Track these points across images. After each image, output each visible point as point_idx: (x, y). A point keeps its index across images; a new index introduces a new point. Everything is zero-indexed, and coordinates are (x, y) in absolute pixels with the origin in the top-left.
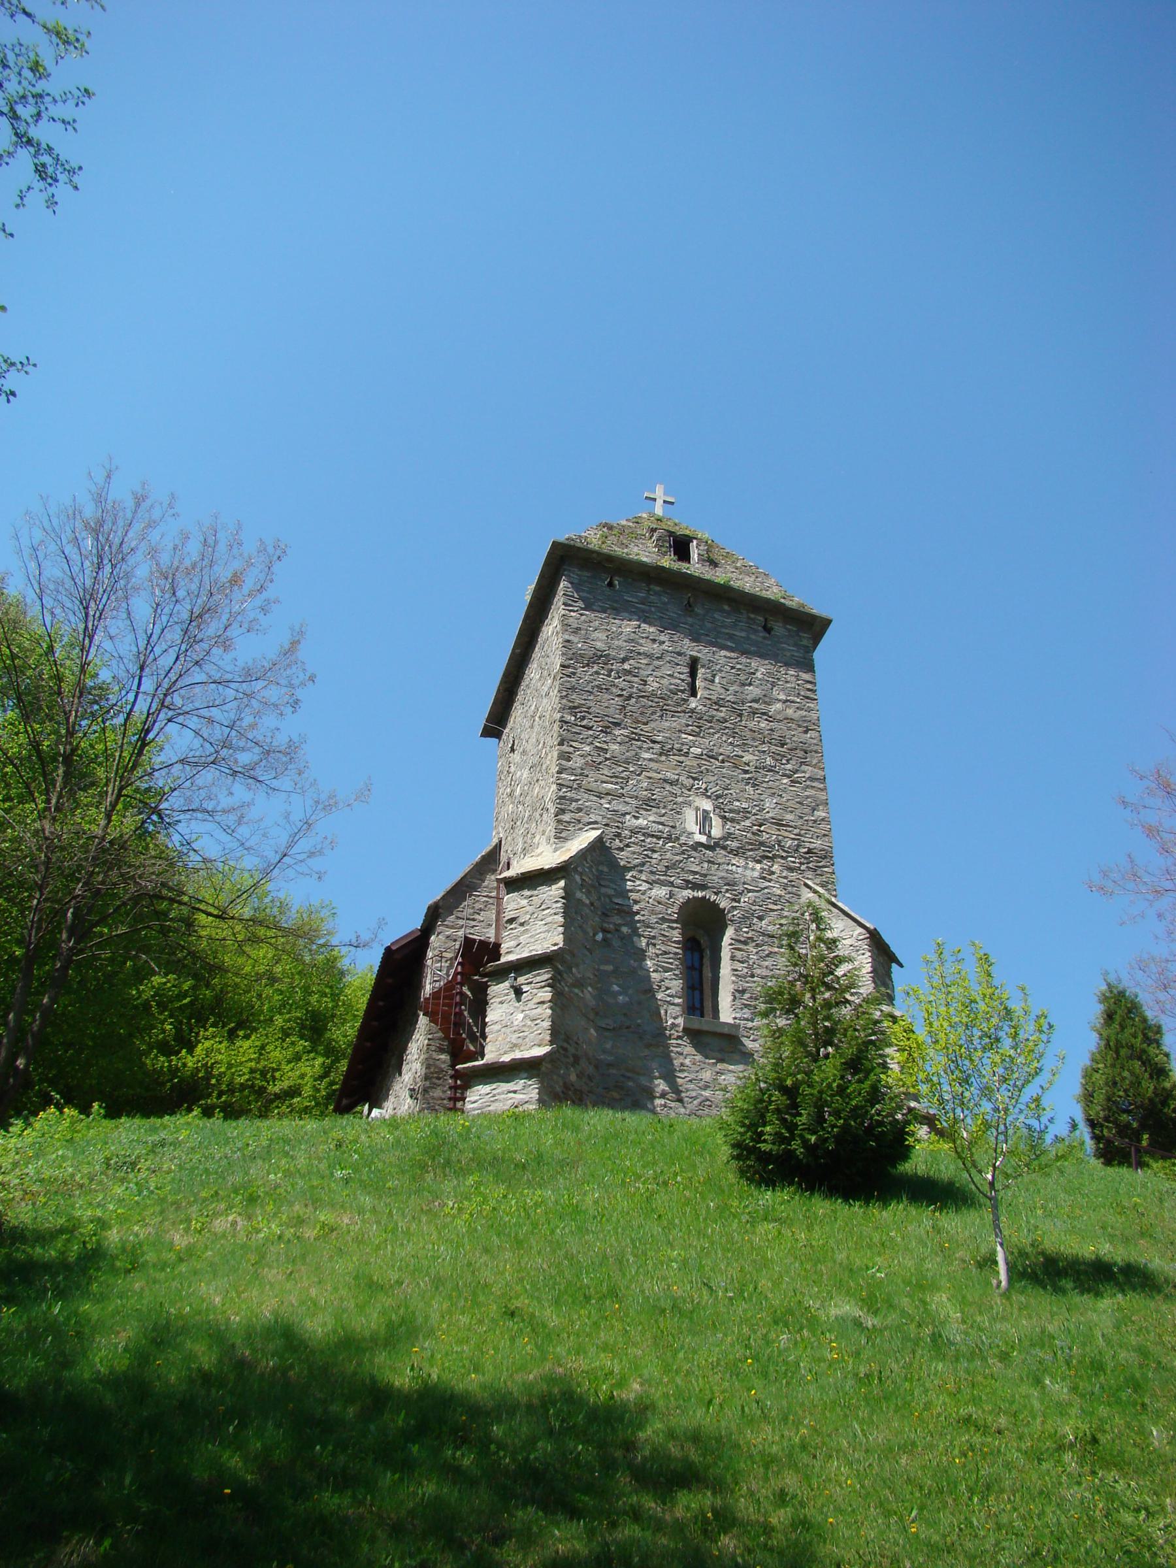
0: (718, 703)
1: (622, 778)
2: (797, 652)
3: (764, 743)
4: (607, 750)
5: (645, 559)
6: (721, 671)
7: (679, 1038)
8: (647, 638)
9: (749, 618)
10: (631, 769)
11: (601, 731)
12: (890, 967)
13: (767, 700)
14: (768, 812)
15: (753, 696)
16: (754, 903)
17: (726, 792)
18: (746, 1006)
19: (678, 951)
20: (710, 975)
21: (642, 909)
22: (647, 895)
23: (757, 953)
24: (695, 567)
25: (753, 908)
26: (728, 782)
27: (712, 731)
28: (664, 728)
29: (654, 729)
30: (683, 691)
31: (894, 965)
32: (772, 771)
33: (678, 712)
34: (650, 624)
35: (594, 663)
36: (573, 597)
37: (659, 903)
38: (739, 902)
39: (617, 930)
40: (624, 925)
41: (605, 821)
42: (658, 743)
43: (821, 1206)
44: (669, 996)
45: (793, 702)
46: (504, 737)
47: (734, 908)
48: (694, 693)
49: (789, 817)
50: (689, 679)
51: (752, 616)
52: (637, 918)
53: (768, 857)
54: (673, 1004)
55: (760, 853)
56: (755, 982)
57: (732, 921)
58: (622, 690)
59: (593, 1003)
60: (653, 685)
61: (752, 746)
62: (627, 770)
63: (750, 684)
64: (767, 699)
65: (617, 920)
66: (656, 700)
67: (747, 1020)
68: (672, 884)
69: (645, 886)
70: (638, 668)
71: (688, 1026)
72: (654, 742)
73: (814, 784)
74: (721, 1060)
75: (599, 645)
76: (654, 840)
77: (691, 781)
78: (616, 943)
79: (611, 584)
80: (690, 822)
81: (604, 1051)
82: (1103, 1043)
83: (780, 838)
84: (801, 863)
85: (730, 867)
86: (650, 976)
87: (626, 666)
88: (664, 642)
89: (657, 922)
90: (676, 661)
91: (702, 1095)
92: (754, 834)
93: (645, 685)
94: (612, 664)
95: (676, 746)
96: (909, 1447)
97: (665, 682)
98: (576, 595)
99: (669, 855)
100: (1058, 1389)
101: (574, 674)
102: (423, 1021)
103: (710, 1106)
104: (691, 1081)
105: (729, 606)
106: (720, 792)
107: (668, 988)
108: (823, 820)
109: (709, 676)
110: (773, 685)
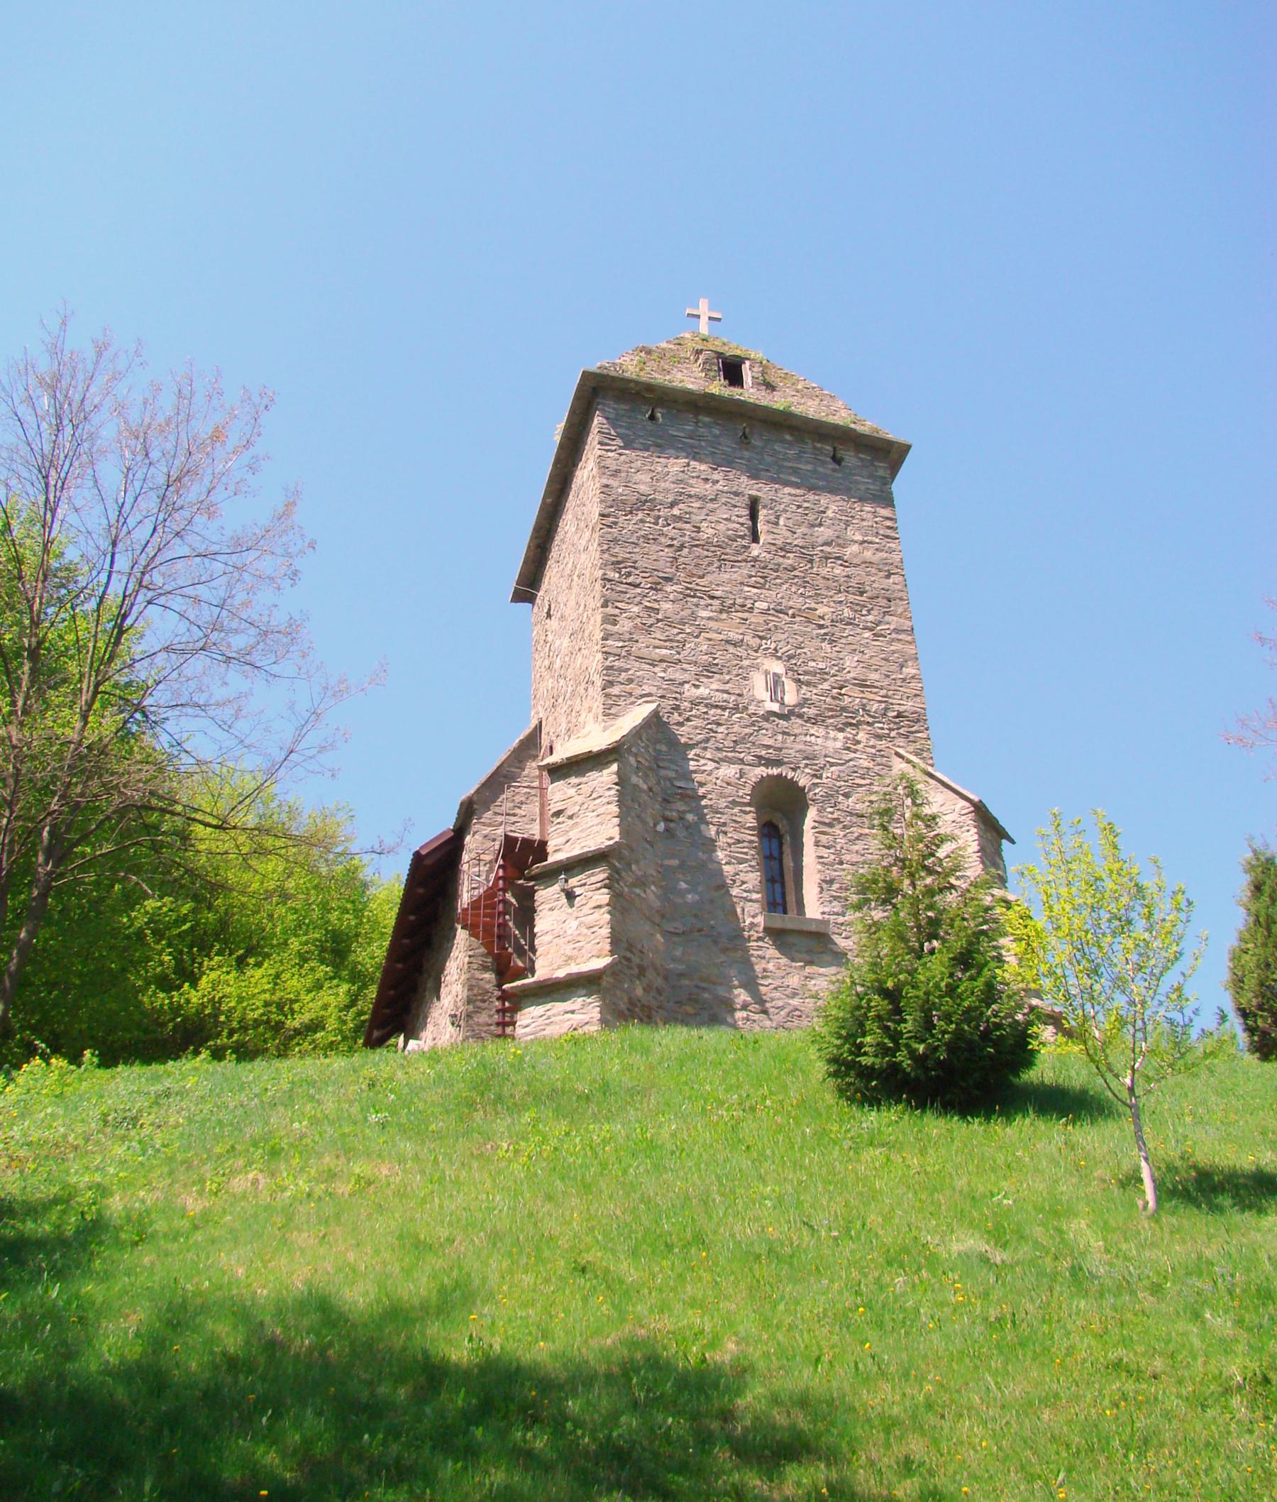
0: (784, 549)
1: (678, 641)
2: (872, 484)
3: (840, 591)
4: (658, 610)
5: (690, 386)
6: (785, 511)
7: (759, 939)
8: (698, 477)
9: (815, 448)
10: (688, 631)
11: (651, 588)
12: (1000, 845)
14: (849, 672)
15: (825, 538)
16: (838, 778)
17: (799, 651)
18: (835, 898)
19: (753, 838)
20: (792, 864)
21: (709, 792)
23: (845, 836)
24: (749, 392)
25: (838, 784)
26: (801, 639)
27: (778, 581)
28: (723, 580)
29: (711, 582)
30: (742, 537)
31: (1004, 842)
32: (851, 624)
34: (701, 461)
35: (638, 509)
36: (610, 434)
37: (728, 784)
38: (820, 777)
39: (681, 818)
40: (689, 811)
41: (660, 692)
42: (717, 598)
43: (936, 1125)
44: (745, 891)
45: (871, 543)
46: (538, 601)
47: (816, 785)
49: (874, 676)
50: (750, 523)
51: (819, 445)
52: (703, 803)
53: (851, 724)
54: (751, 901)
55: (842, 720)
56: (844, 870)
57: (813, 800)
58: (672, 539)
59: (657, 904)
61: (827, 596)
63: (820, 525)
64: (840, 541)
65: (681, 806)
66: (713, 549)
67: (837, 914)
68: (742, 761)
69: (711, 765)
70: (690, 513)
72: (712, 598)
73: (900, 637)
74: (811, 963)
75: (643, 488)
76: (719, 711)
77: (758, 640)
78: (681, 833)
79: (652, 418)
80: (759, 688)
81: (674, 960)
82: (1251, 919)
83: (865, 701)
84: (890, 729)
85: (808, 738)
86: (721, 870)
87: (676, 512)
88: (718, 481)
89: (727, 807)
90: (733, 502)
91: (790, 1004)
92: (833, 698)
93: (698, 532)
94: (659, 510)
95: (739, 601)
96: (1051, 1400)
97: (721, 527)
98: (613, 432)
99: (736, 728)
100: (1220, 1323)
101: (615, 523)
102: (461, 935)
103: (800, 1016)
104: (775, 988)
105: (791, 435)
107: (743, 883)
108: (913, 677)
109: (772, 518)
110: (847, 524)
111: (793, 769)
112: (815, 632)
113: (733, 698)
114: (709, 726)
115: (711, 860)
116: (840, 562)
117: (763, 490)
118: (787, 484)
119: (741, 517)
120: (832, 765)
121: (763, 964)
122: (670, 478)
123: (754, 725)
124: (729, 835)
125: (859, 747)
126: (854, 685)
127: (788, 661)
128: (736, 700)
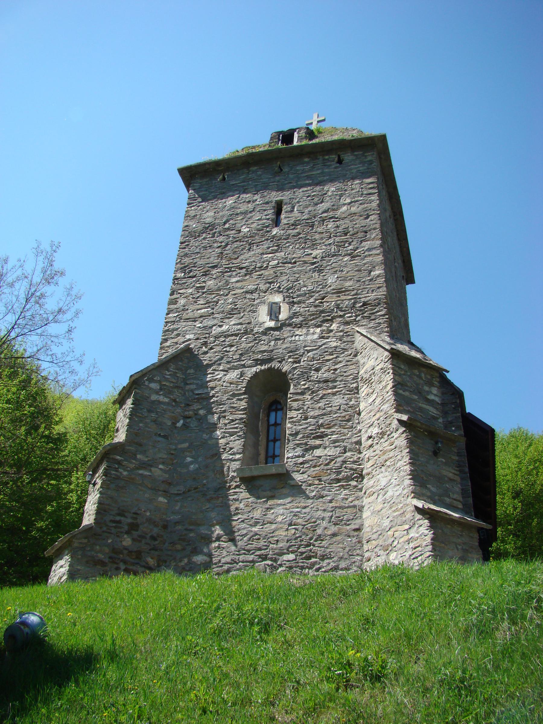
0: (295, 225)
1: (214, 302)
3: (330, 238)
4: (204, 287)
6: (298, 202)
7: (237, 487)
9: (324, 159)
10: (222, 293)
11: (203, 275)
13: (335, 208)
14: (330, 286)
15: (324, 209)
16: (313, 359)
17: (295, 283)
18: (298, 445)
19: (243, 416)
21: (217, 392)
22: (222, 380)
23: (311, 399)
25: (311, 363)
26: (297, 275)
27: (287, 245)
29: (242, 260)
30: (267, 227)
32: (335, 255)
33: (262, 241)
34: (247, 193)
37: (231, 383)
38: (299, 362)
40: (201, 409)
44: (231, 454)
45: (357, 201)
47: (295, 368)
48: (277, 222)
49: (348, 284)
50: (274, 217)
51: (327, 157)
52: (212, 400)
54: (235, 460)
55: (321, 319)
56: (307, 423)
57: (291, 379)
58: (221, 242)
60: (245, 230)
61: (320, 244)
62: (218, 295)
63: (322, 202)
64: (334, 207)
65: (196, 406)
67: (299, 456)
68: (244, 366)
70: (235, 224)
71: (241, 475)
72: (241, 268)
73: (371, 253)
74: (272, 497)
75: (208, 220)
77: (268, 285)
78: (193, 424)
79: (224, 179)
83: (339, 302)
84: (356, 316)
85: (293, 338)
86: (218, 443)
87: (227, 226)
88: (256, 200)
89: (228, 399)
90: (264, 208)
92: (316, 306)
94: (216, 229)
95: (259, 265)
98: (197, 196)
103: (259, 539)
104: (243, 521)
105: (309, 157)
106: (291, 285)
107: (231, 449)
109: (289, 209)
110: (341, 196)
111: (280, 362)
112: (308, 268)
113: (244, 326)
114: (225, 349)
115: (211, 438)
116: (332, 220)
117: (285, 196)
118: (300, 187)
119: (268, 215)
120: (309, 351)
121: (237, 504)
122: (227, 208)
123: (256, 340)
124: (227, 418)
125: (331, 334)
126: (333, 293)
127: (287, 292)
128: (246, 327)
